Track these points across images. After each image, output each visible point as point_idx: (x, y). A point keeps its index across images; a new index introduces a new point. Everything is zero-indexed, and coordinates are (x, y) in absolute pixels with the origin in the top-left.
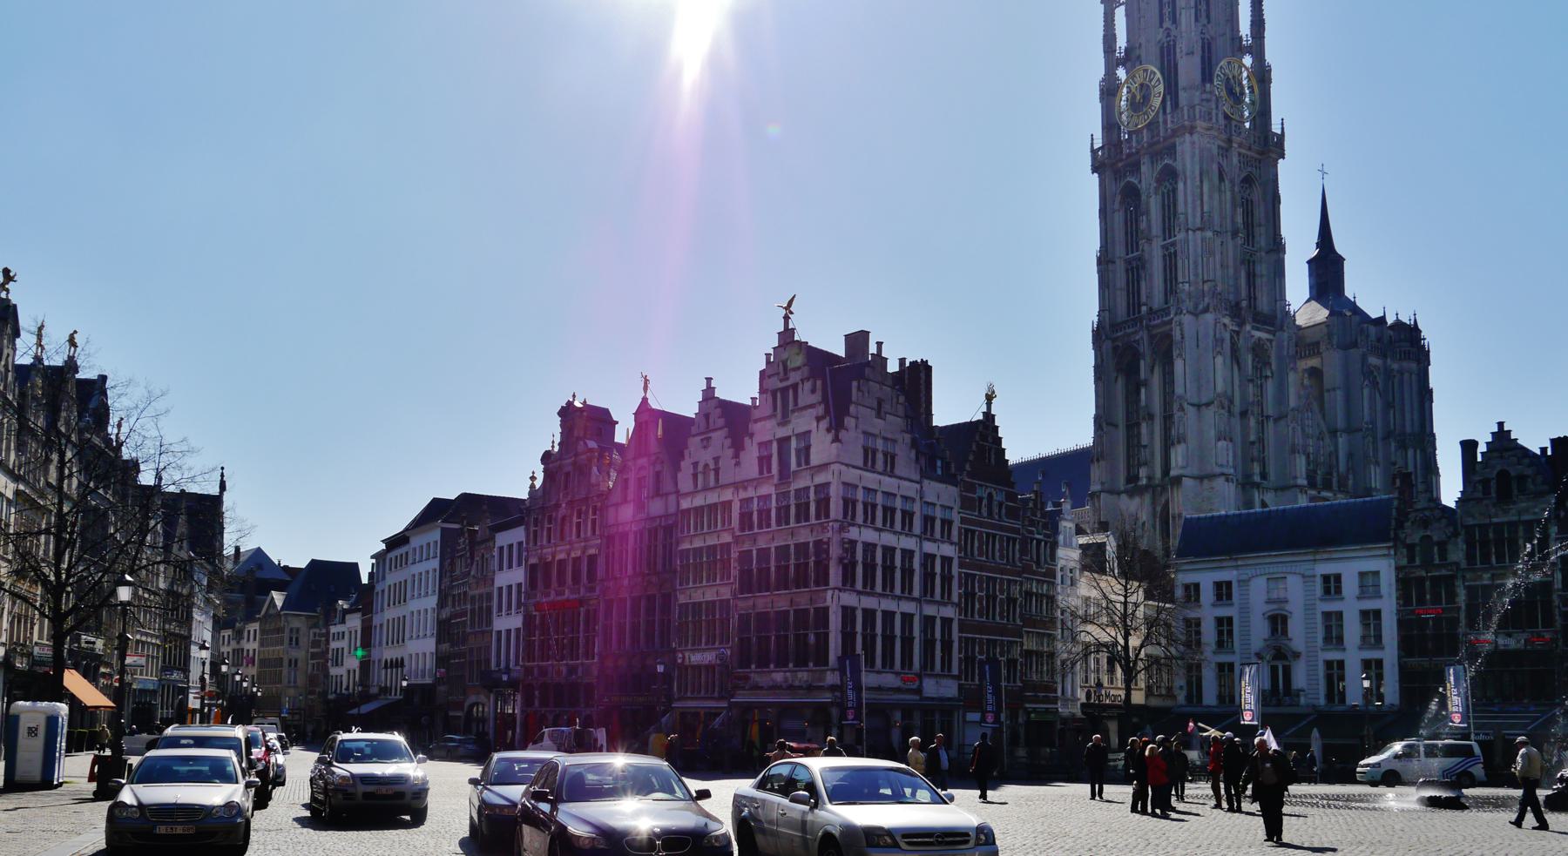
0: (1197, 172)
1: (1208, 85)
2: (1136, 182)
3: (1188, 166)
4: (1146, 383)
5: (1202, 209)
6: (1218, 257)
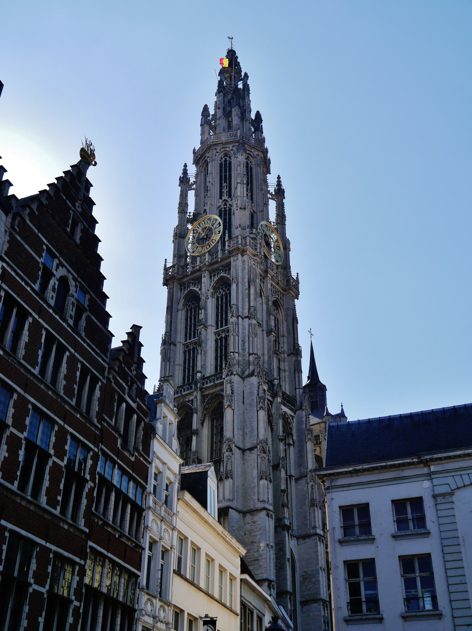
0: (246, 280)
2: (197, 290)
3: (240, 275)
4: (196, 433)
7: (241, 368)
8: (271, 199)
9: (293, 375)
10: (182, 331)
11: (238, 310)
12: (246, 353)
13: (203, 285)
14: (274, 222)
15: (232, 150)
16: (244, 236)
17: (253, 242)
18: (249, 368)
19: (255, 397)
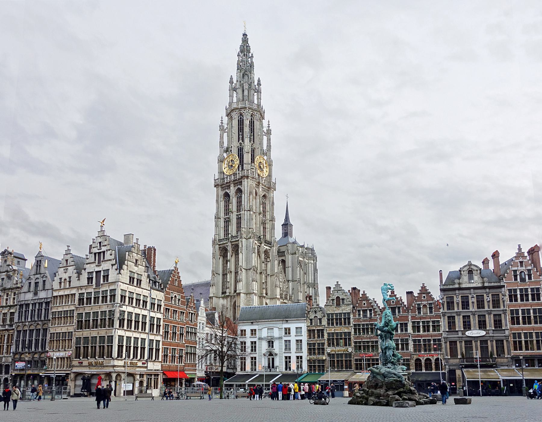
0: (249, 192)
1: (253, 164)
2: (229, 192)
5: (250, 204)
6: (254, 220)
13: (231, 191)
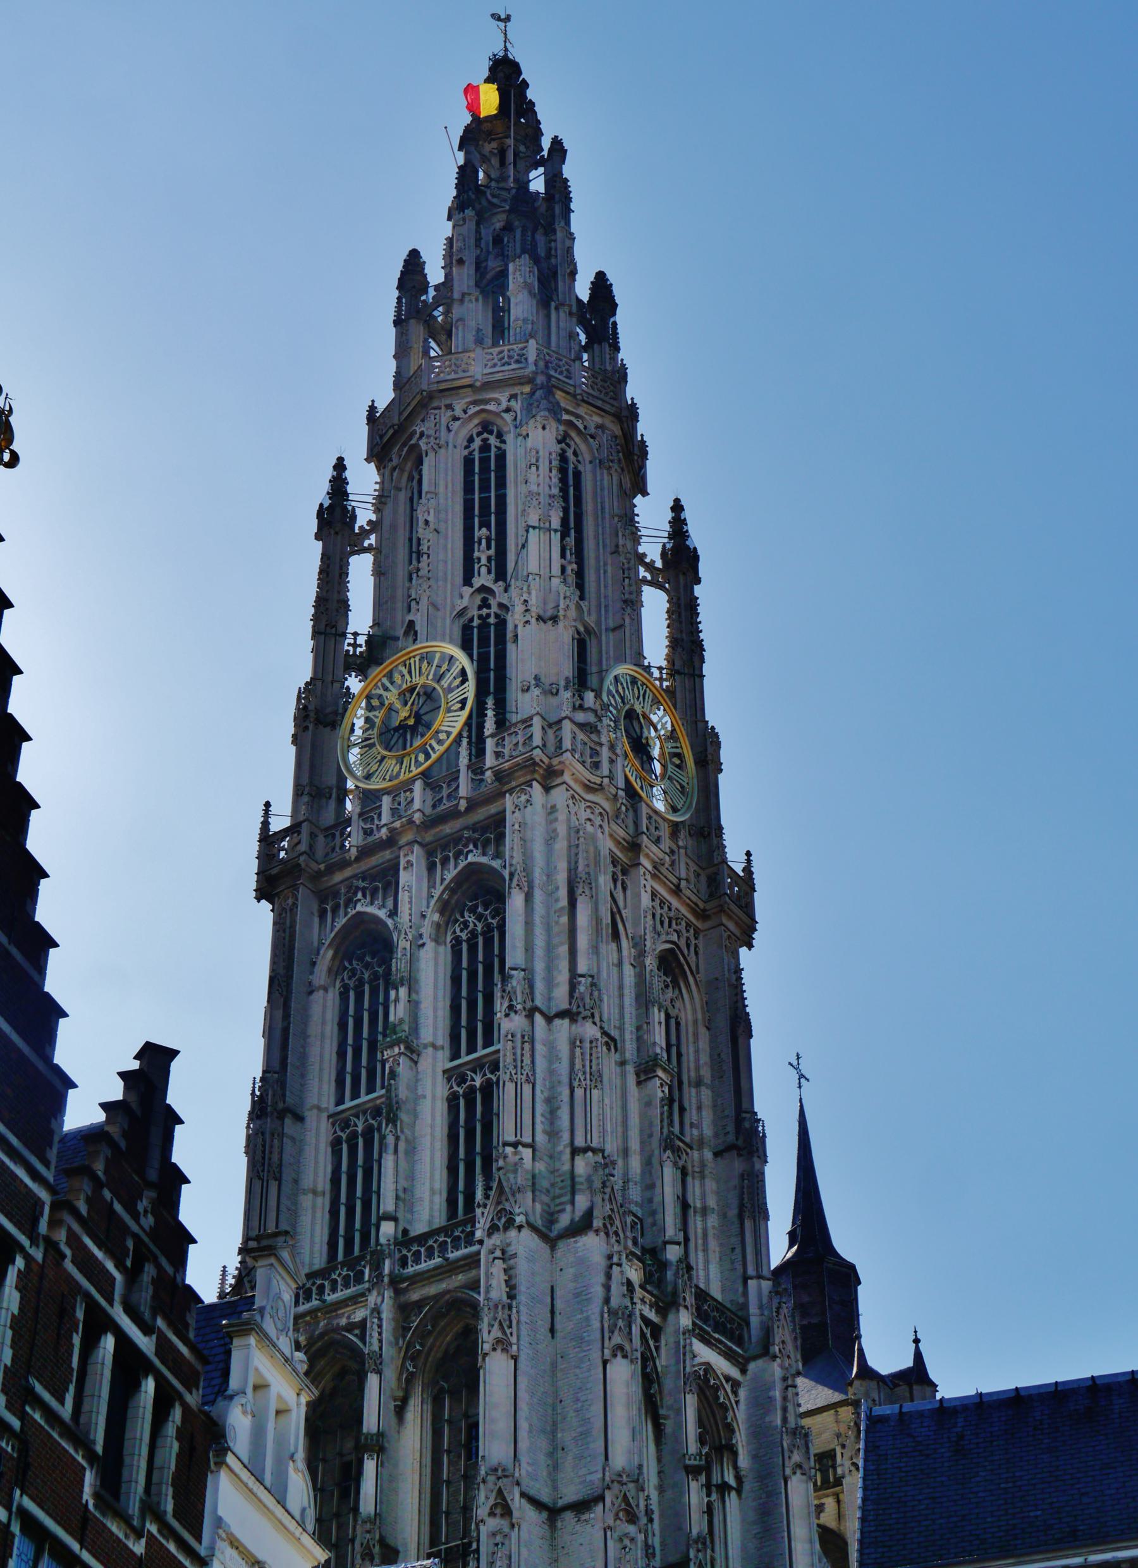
0: (562, 878)
2: (382, 914)
4: (379, 1446)
7: (542, 1203)
8: (653, 583)
9: (735, 1228)
10: (326, 1065)
11: (531, 986)
12: (561, 1148)
13: (403, 896)
14: (660, 668)
15: (508, 410)
16: (553, 719)
17: (586, 739)
18: (573, 1203)
19: (595, 1308)
